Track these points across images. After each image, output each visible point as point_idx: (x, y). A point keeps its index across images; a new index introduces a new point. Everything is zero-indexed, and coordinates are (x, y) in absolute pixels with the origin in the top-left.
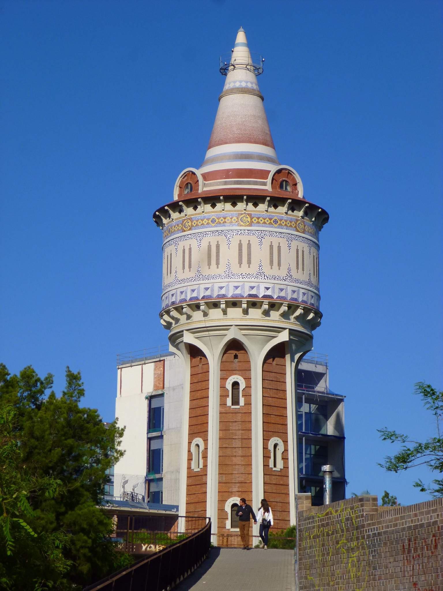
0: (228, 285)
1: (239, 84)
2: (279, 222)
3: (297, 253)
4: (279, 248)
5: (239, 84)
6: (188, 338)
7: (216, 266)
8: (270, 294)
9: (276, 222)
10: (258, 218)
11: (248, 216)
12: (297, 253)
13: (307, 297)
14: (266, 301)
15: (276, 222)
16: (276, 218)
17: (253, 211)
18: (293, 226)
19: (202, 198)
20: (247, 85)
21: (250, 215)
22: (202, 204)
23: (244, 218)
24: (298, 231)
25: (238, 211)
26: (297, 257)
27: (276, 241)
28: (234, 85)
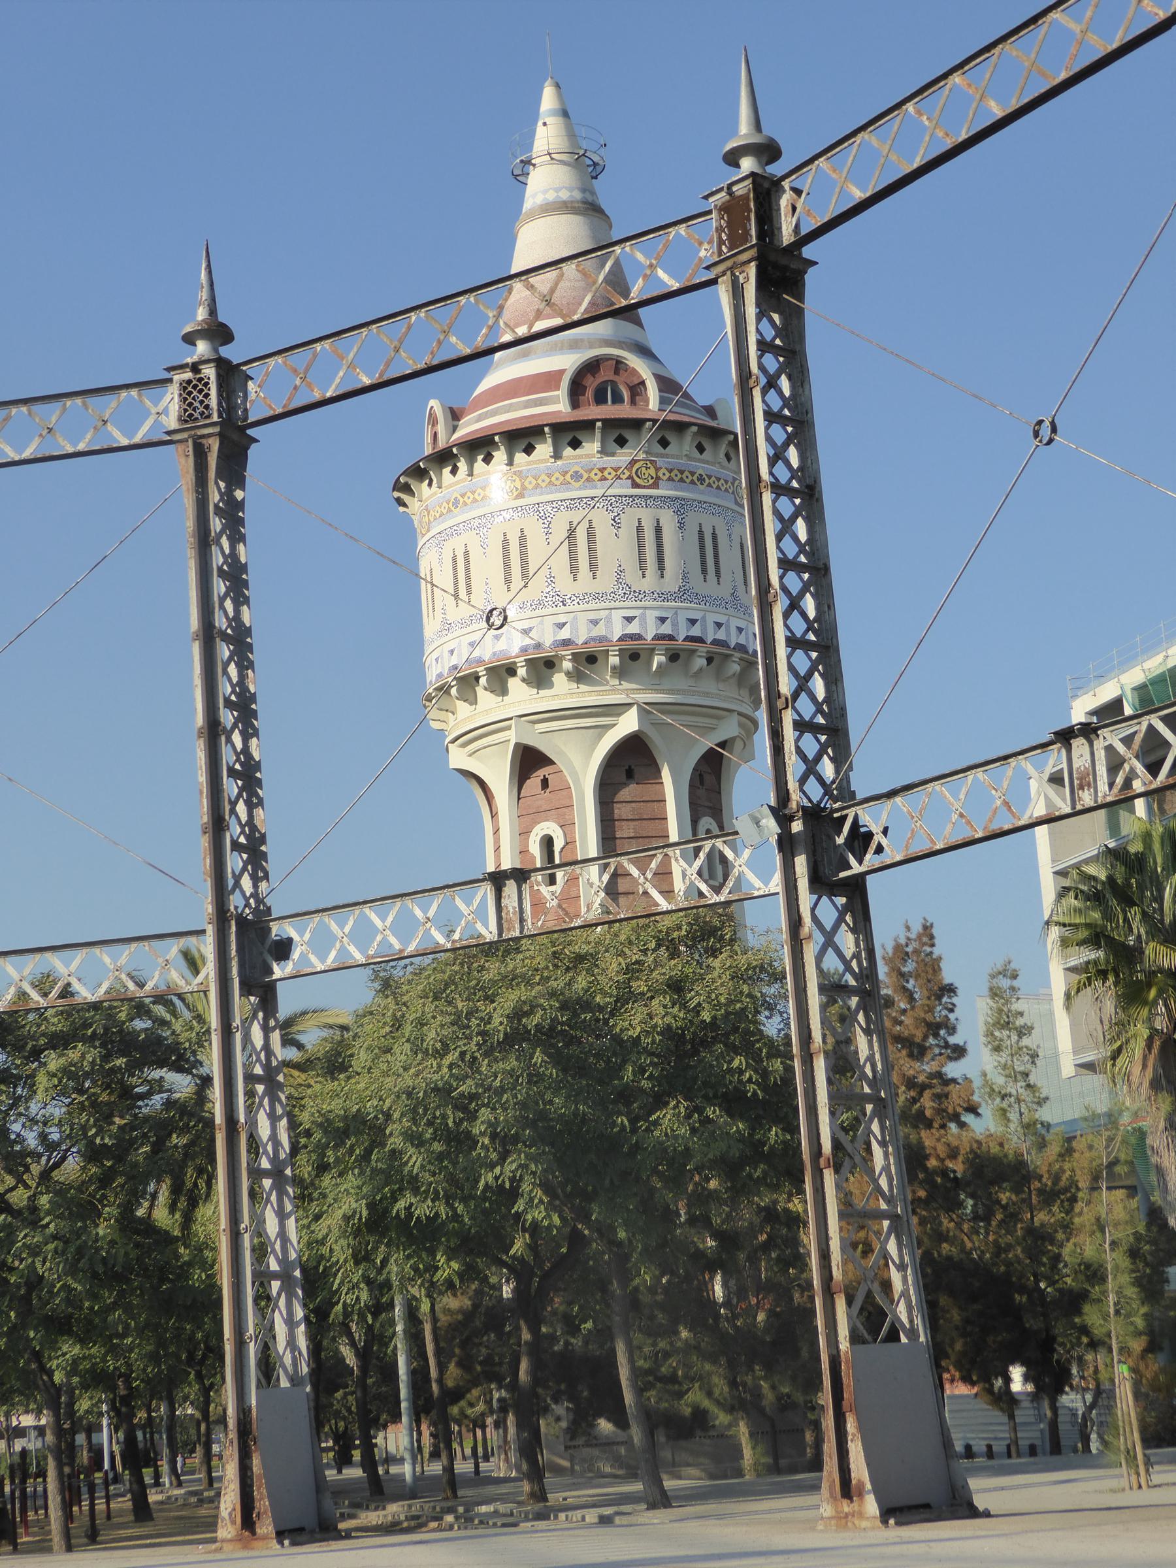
0: (575, 618)
16: (700, 471)
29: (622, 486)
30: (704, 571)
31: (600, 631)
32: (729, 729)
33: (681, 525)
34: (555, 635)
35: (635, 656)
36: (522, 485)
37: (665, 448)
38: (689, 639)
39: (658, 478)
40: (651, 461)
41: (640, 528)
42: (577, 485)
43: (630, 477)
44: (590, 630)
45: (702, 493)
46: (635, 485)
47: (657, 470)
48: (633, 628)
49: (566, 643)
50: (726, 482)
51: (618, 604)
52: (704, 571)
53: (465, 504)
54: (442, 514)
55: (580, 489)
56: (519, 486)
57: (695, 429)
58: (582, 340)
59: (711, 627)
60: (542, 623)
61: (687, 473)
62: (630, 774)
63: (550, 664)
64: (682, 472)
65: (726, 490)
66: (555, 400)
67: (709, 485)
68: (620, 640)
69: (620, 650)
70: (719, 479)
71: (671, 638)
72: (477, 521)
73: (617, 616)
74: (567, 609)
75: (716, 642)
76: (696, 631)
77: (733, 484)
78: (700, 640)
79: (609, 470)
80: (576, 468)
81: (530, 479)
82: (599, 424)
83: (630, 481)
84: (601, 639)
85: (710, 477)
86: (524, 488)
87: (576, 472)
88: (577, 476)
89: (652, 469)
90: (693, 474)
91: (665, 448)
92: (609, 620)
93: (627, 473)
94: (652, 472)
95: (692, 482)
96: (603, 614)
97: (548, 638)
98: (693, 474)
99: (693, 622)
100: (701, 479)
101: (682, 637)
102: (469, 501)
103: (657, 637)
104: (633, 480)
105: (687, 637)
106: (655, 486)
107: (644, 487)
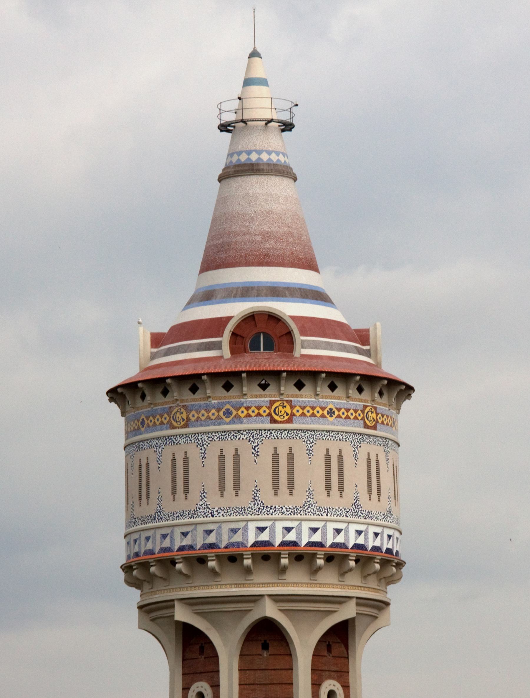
1: (247, 157)
2: (337, 413)
4: (340, 458)
5: (247, 157)
6: (181, 614)
8: (267, 539)
10: (313, 408)
11: (286, 404)
14: (210, 553)
15: (331, 412)
16: (331, 406)
18: (360, 418)
19: (207, 374)
22: (208, 385)
23: (281, 408)
28: (249, 159)
29: (262, 422)
30: (328, 488)
31: (238, 538)
32: (348, 612)
34: (204, 540)
35: (266, 557)
36: (188, 417)
37: (300, 390)
39: (293, 415)
41: (276, 455)
42: (228, 420)
43: (269, 415)
44: (230, 538)
45: (332, 424)
46: (273, 421)
47: (292, 407)
48: (264, 537)
49: (212, 546)
50: (356, 411)
51: (253, 517)
52: (328, 488)
53: (148, 425)
54: (134, 430)
55: (230, 423)
56: (185, 418)
57: (324, 375)
58: (252, 288)
60: (195, 529)
61: (318, 409)
62: (265, 647)
63: (202, 560)
64: (313, 408)
65: (355, 418)
67: (339, 416)
68: (253, 545)
69: (252, 554)
70: (348, 410)
71: (294, 544)
72: (154, 442)
73: (252, 527)
74: (214, 519)
75: (334, 545)
76: (317, 538)
77: (363, 411)
78: (320, 545)
79: (253, 408)
80: (228, 406)
81: (193, 412)
82: (244, 375)
83: (269, 418)
84: (238, 545)
85: (339, 410)
86: (188, 420)
87: (228, 410)
88: (228, 413)
89: (288, 407)
90: (323, 409)
91: (300, 390)
92: (246, 529)
93: (268, 411)
94: (288, 409)
95: (323, 416)
96: (242, 525)
97: (199, 540)
98: (323, 409)
99: (314, 530)
100: (331, 412)
101: (304, 542)
102: (151, 424)
103: (283, 544)
104: (272, 417)
105: (309, 542)
106: (290, 421)
107: (280, 422)
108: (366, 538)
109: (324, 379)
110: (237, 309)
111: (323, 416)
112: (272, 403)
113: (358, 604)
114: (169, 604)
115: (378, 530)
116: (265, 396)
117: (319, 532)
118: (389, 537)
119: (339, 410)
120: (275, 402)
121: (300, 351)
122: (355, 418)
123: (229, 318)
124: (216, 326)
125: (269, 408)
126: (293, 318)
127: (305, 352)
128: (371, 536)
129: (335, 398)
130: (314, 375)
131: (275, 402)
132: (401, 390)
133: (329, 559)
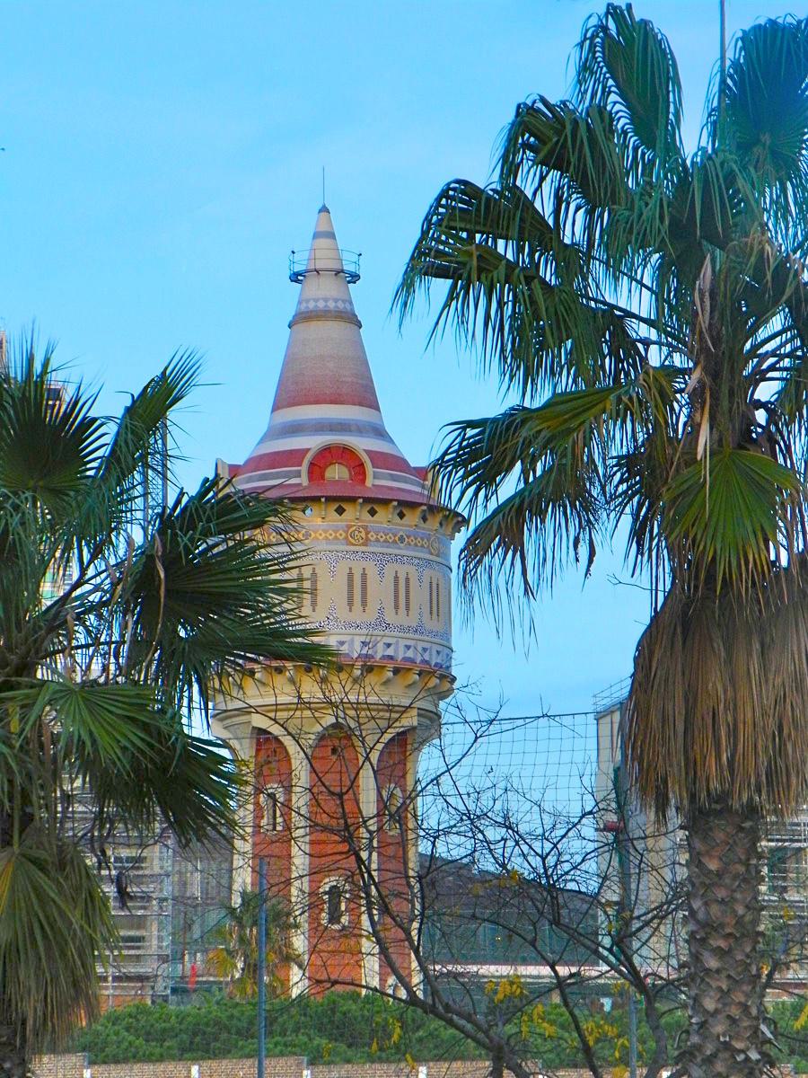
1: (334, 304)
3: (431, 587)
4: (407, 580)
7: (361, 608)
9: (402, 539)
12: (431, 587)
13: (431, 655)
15: (402, 539)
16: (401, 533)
17: (370, 522)
20: (337, 307)
21: (365, 528)
24: (432, 554)
25: (347, 521)
26: (431, 591)
27: (403, 571)
32: (411, 720)
33: (381, 574)
38: (384, 657)
39: (367, 539)
40: (362, 526)
41: (350, 575)
43: (346, 538)
47: (367, 533)
52: (397, 607)
59: (402, 649)
66: (298, 474)
75: (405, 659)
82: (323, 500)
94: (363, 535)
106: (366, 542)
108: (431, 655)
109: (395, 507)
110: (313, 443)
111: (395, 542)
112: (349, 527)
113: (419, 715)
114: (247, 710)
115: (426, 645)
116: (341, 521)
117: (392, 647)
118: (438, 652)
119: (408, 537)
120: (352, 526)
121: (370, 482)
122: (422, 546)
123: (308, 450)
124: (294, 457)
125: (346, 532)
126: (367, 452)
127: (378, 482)
128: (434, 653)
129: (402, 525)
130: (385, 502)
131: (352, 526)
132: (458, 522)
133: (396, 671)
